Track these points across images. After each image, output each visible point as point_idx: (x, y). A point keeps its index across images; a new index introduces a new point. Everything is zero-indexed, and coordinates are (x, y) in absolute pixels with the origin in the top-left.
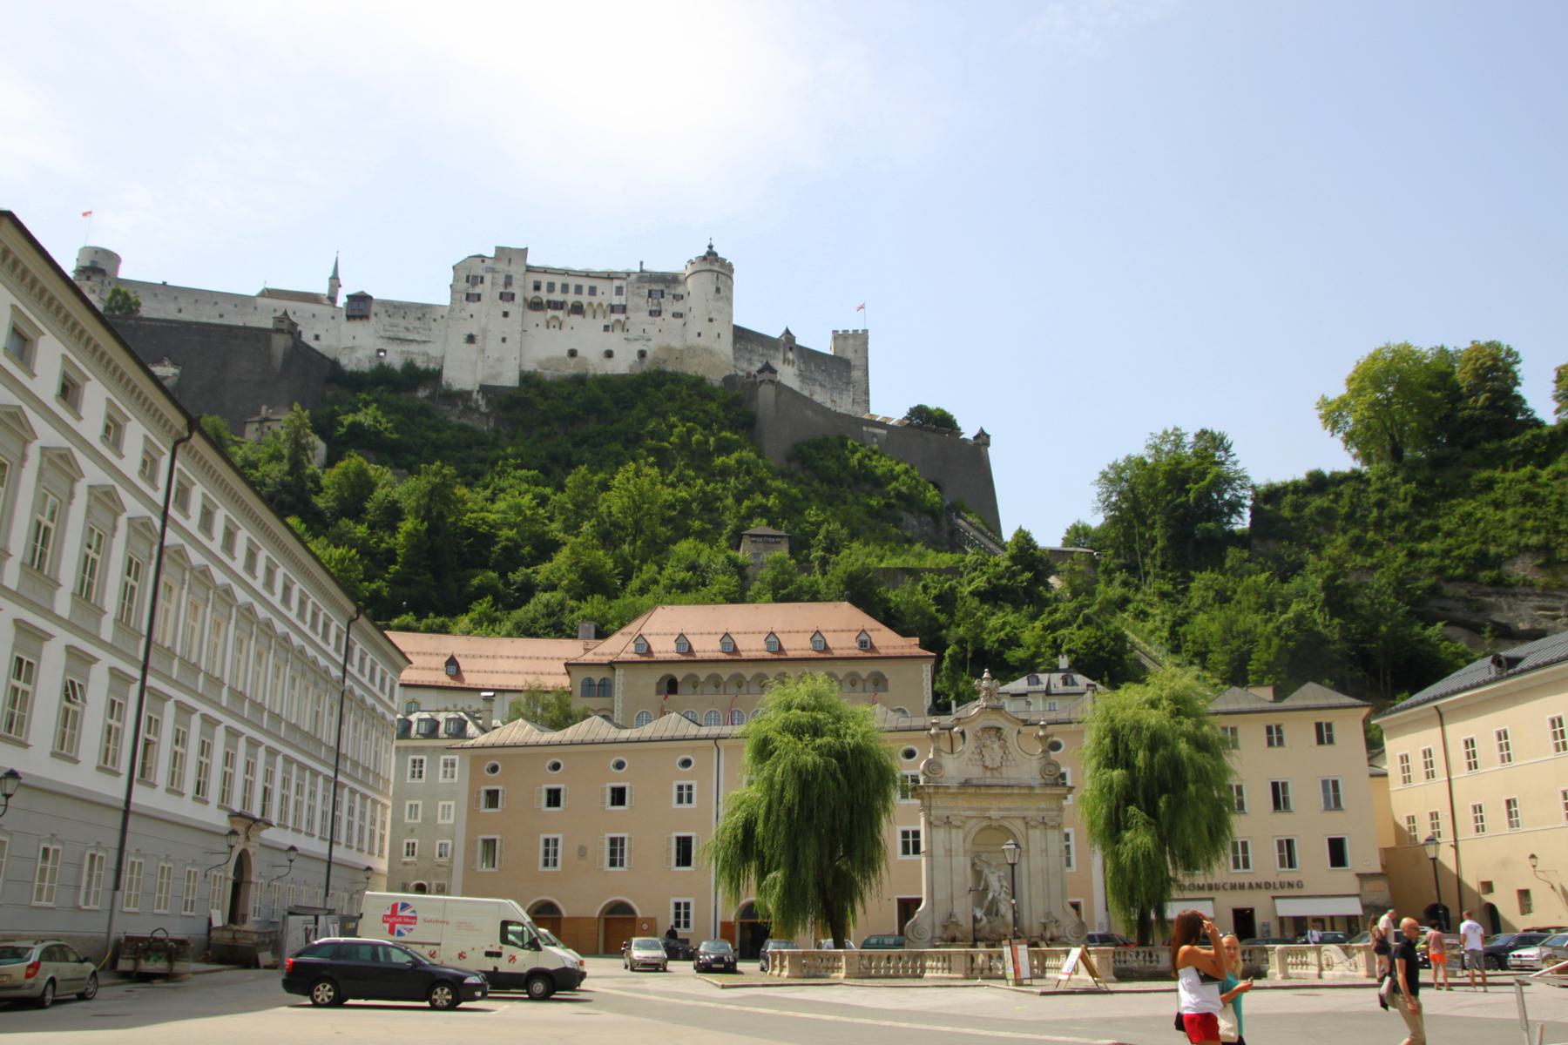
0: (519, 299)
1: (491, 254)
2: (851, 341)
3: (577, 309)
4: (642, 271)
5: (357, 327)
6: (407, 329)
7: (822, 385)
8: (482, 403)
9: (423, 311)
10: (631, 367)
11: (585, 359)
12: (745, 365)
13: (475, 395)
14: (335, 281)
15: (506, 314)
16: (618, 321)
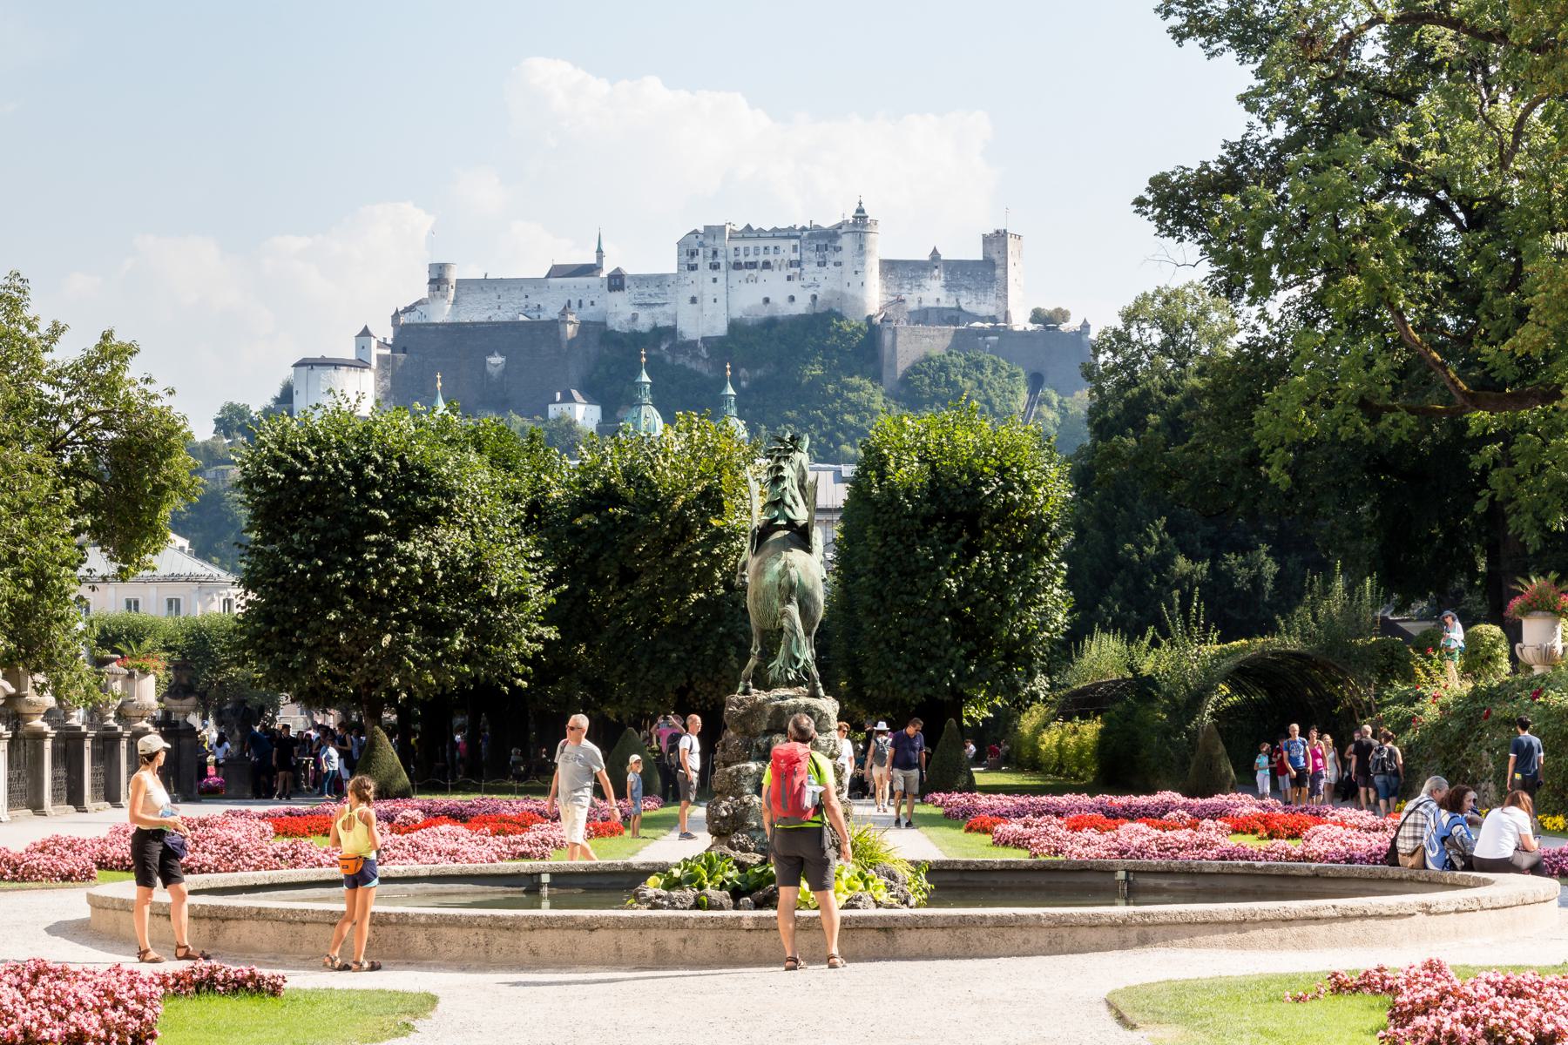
1: (701, 229)
3: (767, 265)
5: (617, 295)
7: (968, 289)
8: (704, 351)
9: (660, 280)
14: (599, 251)
15: (715, 280)
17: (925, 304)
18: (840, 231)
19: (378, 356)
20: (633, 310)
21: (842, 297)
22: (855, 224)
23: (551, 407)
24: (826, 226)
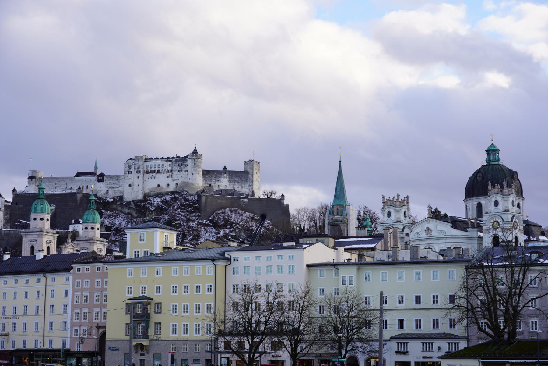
0: (142, 173)
1: (134, 158)
2: (249, 165)
3: (159, 172)
4: (176, 158)
5: (101, 184)
6: (114, 184)
7: (238, 182)
8: (133, 205)
9: (118, 177)
10: (174, 189)
11: (162, 187)
12: (209, 182)
13: (132, 202)
14: (96, 167)
15: (138, 177)
16: (170, 175)
17: (221, 188)
18: (187, 158)
19: (5, 206)
20: (107, 189)
21: (186, 184)
22: (193, 155)
23: (71, 226)
24: (182, 156)
